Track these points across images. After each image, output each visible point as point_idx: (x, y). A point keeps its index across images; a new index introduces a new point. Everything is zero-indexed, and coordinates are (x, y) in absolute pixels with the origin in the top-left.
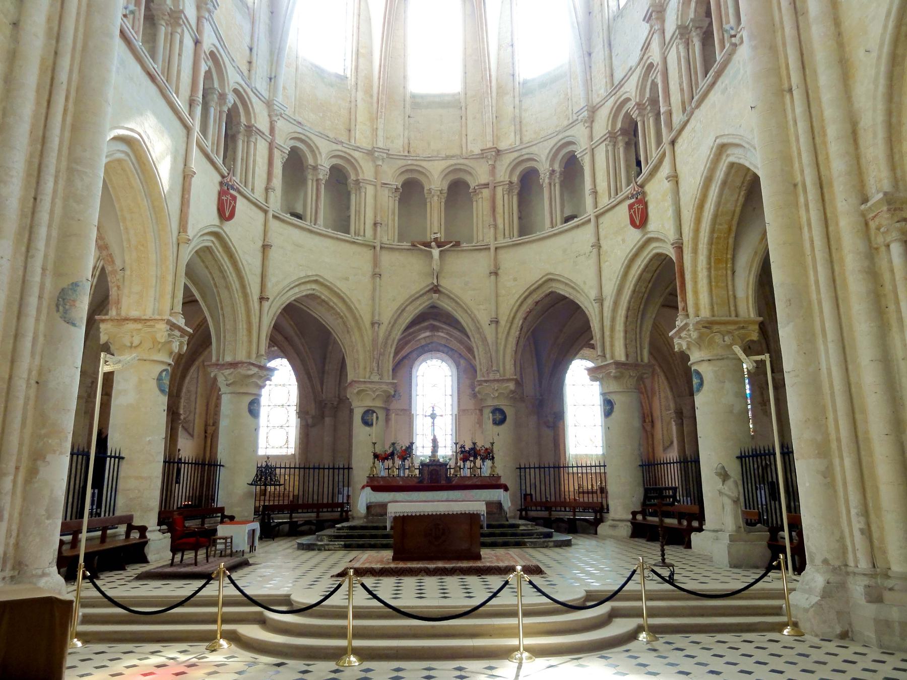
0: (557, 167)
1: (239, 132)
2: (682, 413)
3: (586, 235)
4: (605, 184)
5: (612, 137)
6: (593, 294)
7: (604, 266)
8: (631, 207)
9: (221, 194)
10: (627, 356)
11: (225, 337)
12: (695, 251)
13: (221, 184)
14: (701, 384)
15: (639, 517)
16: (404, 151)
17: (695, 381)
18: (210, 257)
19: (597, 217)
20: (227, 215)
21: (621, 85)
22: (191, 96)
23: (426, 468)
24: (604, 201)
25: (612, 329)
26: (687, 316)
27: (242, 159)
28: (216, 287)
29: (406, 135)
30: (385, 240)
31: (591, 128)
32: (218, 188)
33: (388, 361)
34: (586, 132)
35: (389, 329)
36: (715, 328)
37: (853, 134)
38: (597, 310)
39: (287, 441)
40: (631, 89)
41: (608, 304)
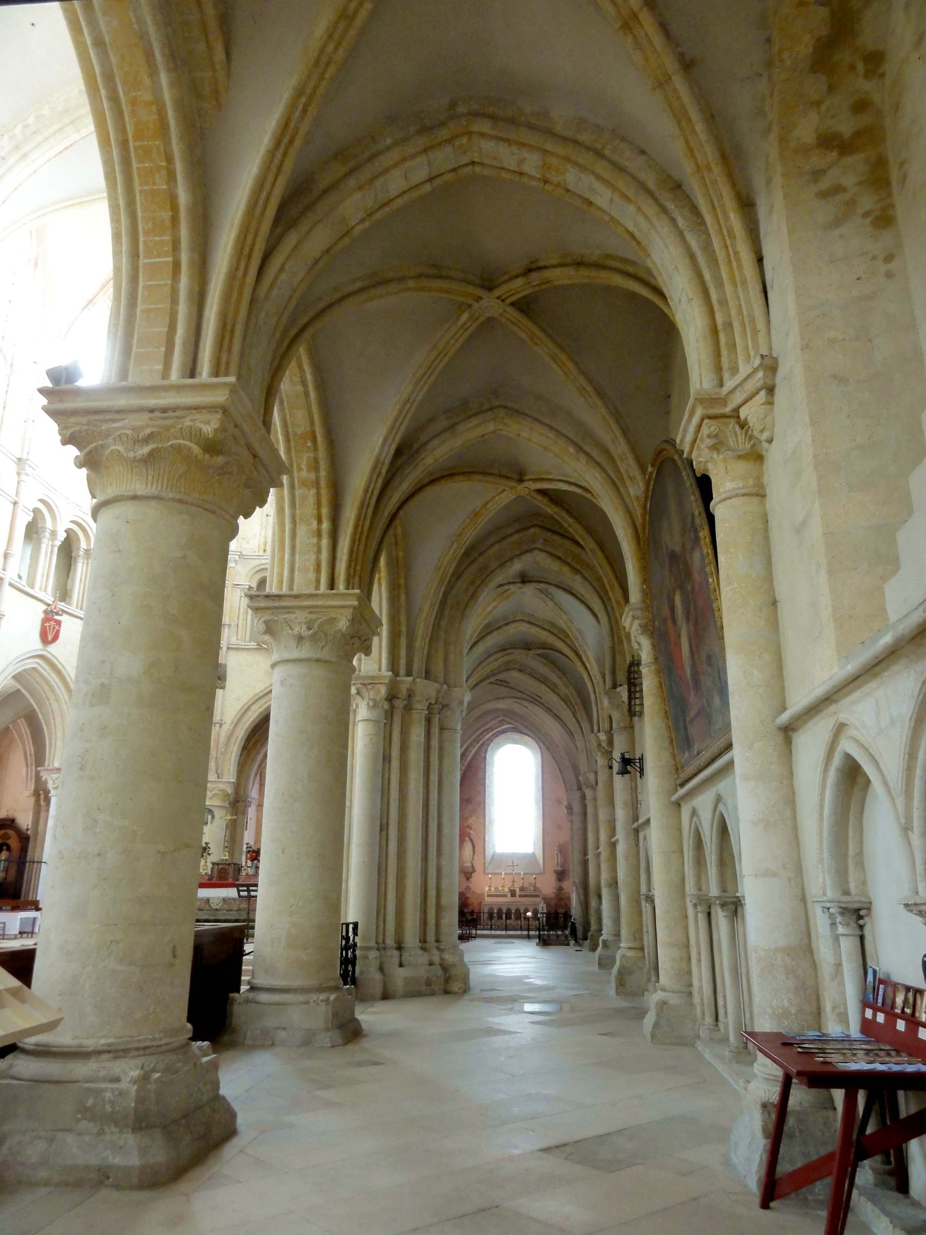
1: (79, 556)
2: (572, 809)
9: (46, 620)
11: (55, 744)
13: (45, 612)
16: (259, 551)
18: (37, 675)
20: (50, 638)
22: (7, 549)
23: (216, 867)
27: (81, 580)
28: (48, 700)
29: (263, 534)
30: (234, 640)
32: (43, 616)
33: (230, 759)
35: (231, 728)
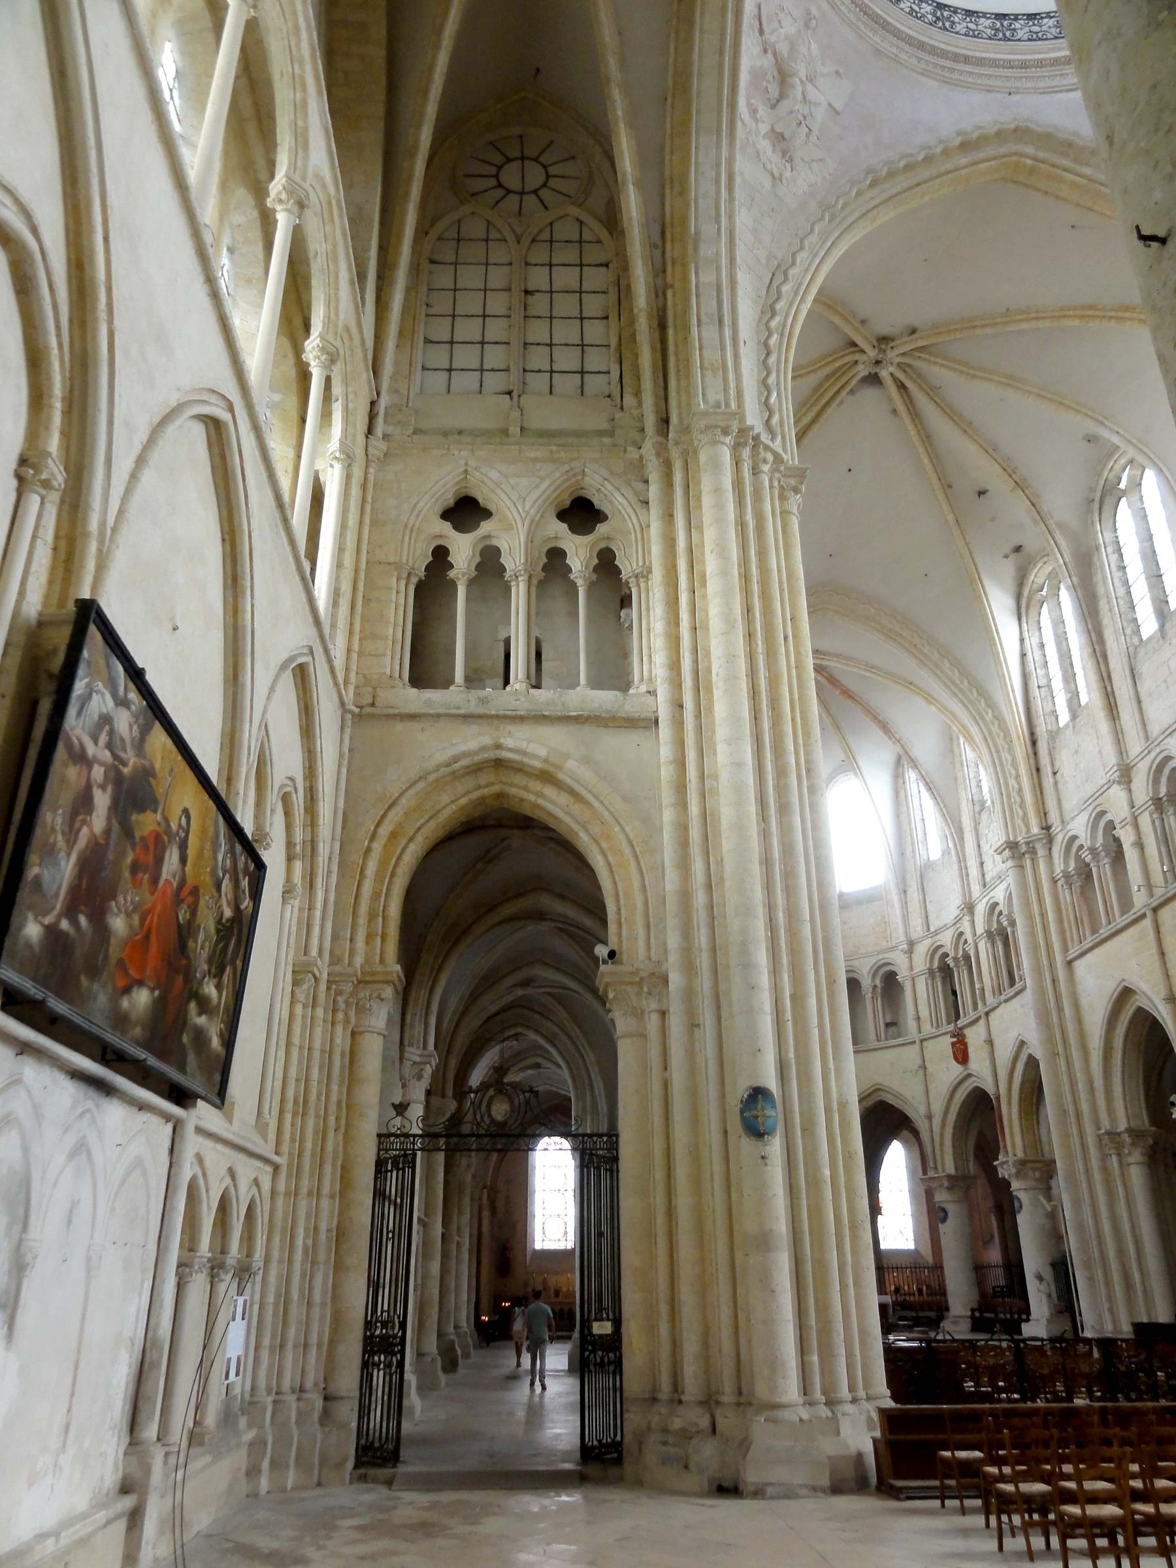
0: (878, 982)
3: (910, 1055)
4: (928, 1013)
5: (931, 972)
6: (922, 1110)
7: (931, 1087)
8: (953, 1044)
10: (956, 1169)
12: (1009, 1103)
14: (1021, 1206)
15: (977, 1314)
17: (1016, 1204)
19: (922, 1041)
21: (936, 933)
24: (927, 1029)
25: (942, 1144)
26: (1007, 1152)
31: (910, 958)
34: (906, 961)
36: (1029, 1165)
37: (1091, 1090)
38: (927, 1125)
39: (566, 1233)
40: (947, 939)
41: (937, 1121)
